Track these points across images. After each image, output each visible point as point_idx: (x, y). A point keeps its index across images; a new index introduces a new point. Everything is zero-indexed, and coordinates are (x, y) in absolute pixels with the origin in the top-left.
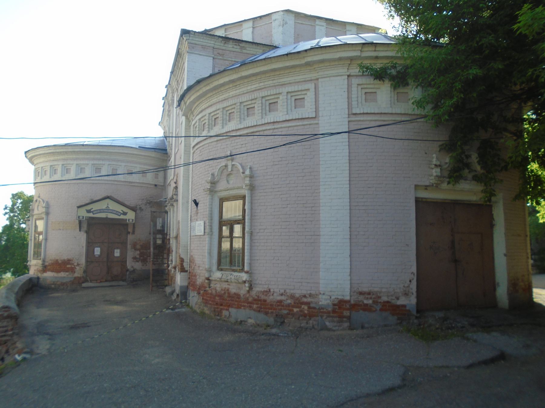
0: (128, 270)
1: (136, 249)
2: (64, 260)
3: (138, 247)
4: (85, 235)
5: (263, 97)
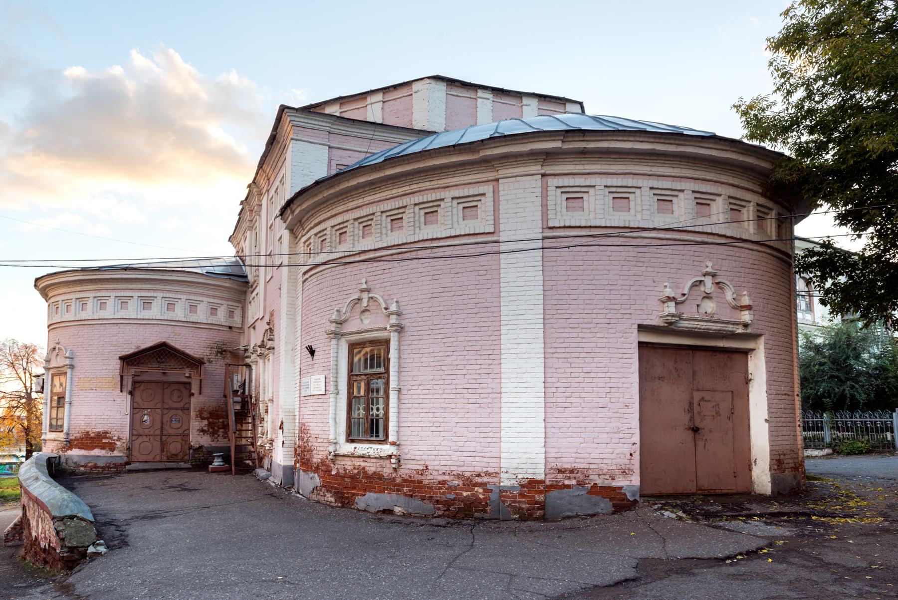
0: (190, 447)
1: (203, 418)
2: (99, 432)
3: (205, 415)
4: (129, 396)
5: (415, 205)
